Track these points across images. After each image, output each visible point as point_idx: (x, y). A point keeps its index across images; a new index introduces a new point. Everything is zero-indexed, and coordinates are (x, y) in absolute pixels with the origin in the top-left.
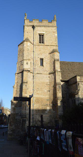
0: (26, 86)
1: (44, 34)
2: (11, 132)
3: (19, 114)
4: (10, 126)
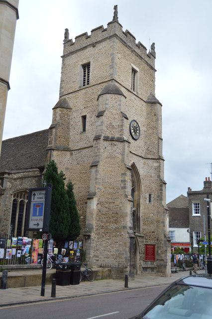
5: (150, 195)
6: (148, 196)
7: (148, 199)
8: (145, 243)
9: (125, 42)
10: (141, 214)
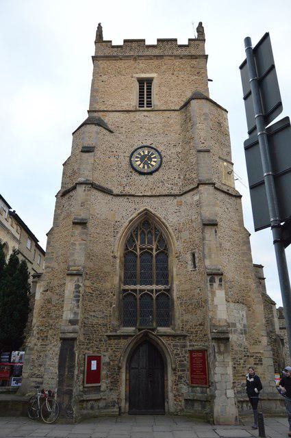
3: (239, 327)
5: (193, 255)
6: (189, 257)
7: (190, 262)
8: (189, 348)
9: (114, 57)
10: (175, 294)
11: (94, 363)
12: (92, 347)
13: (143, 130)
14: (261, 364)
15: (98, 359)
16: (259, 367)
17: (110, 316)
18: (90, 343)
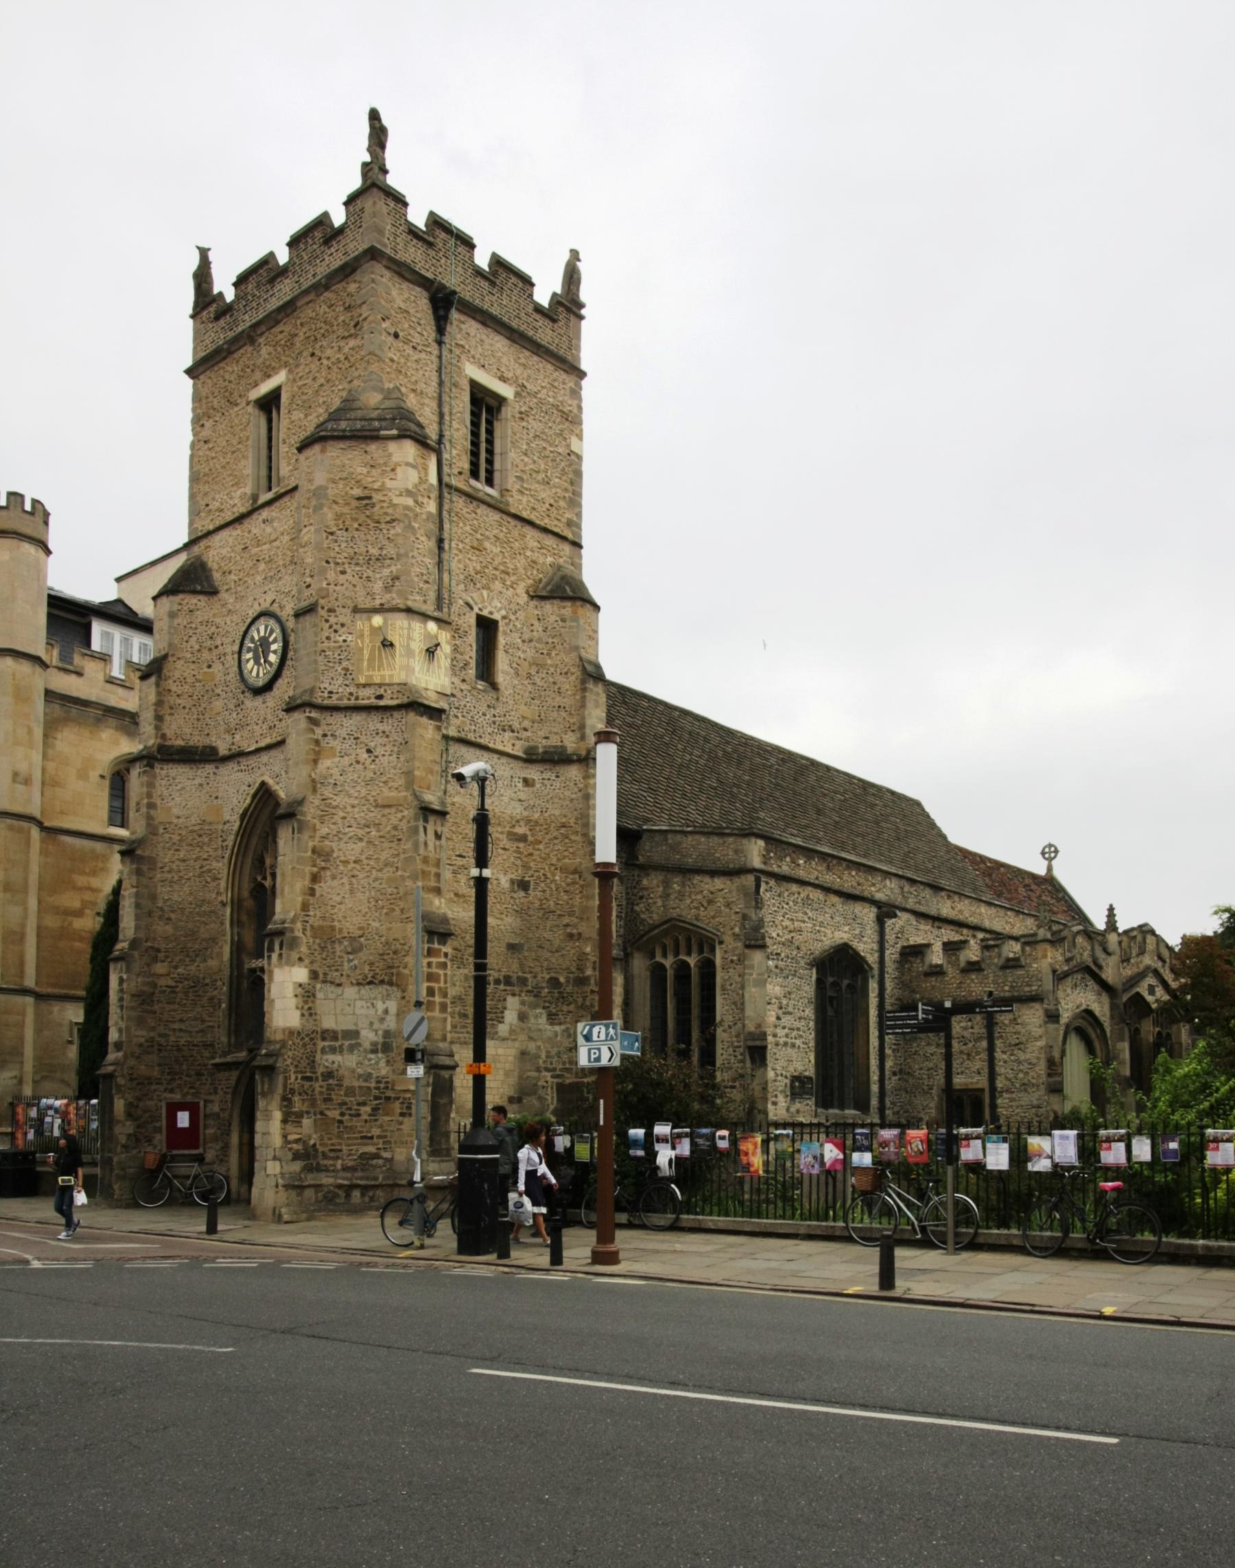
0: (438, 836)
1: (501, 400)
2: (297, 1166)
3: (368, 1037)
4: (284, 1121)
11: (183, 1119)
12: (179, 1086)
13: (262, 566)
14: (410, 1115)
15: (193, 1109)
16: (406, 1120)
17: (219, 1027)
18: (173, 1079)
